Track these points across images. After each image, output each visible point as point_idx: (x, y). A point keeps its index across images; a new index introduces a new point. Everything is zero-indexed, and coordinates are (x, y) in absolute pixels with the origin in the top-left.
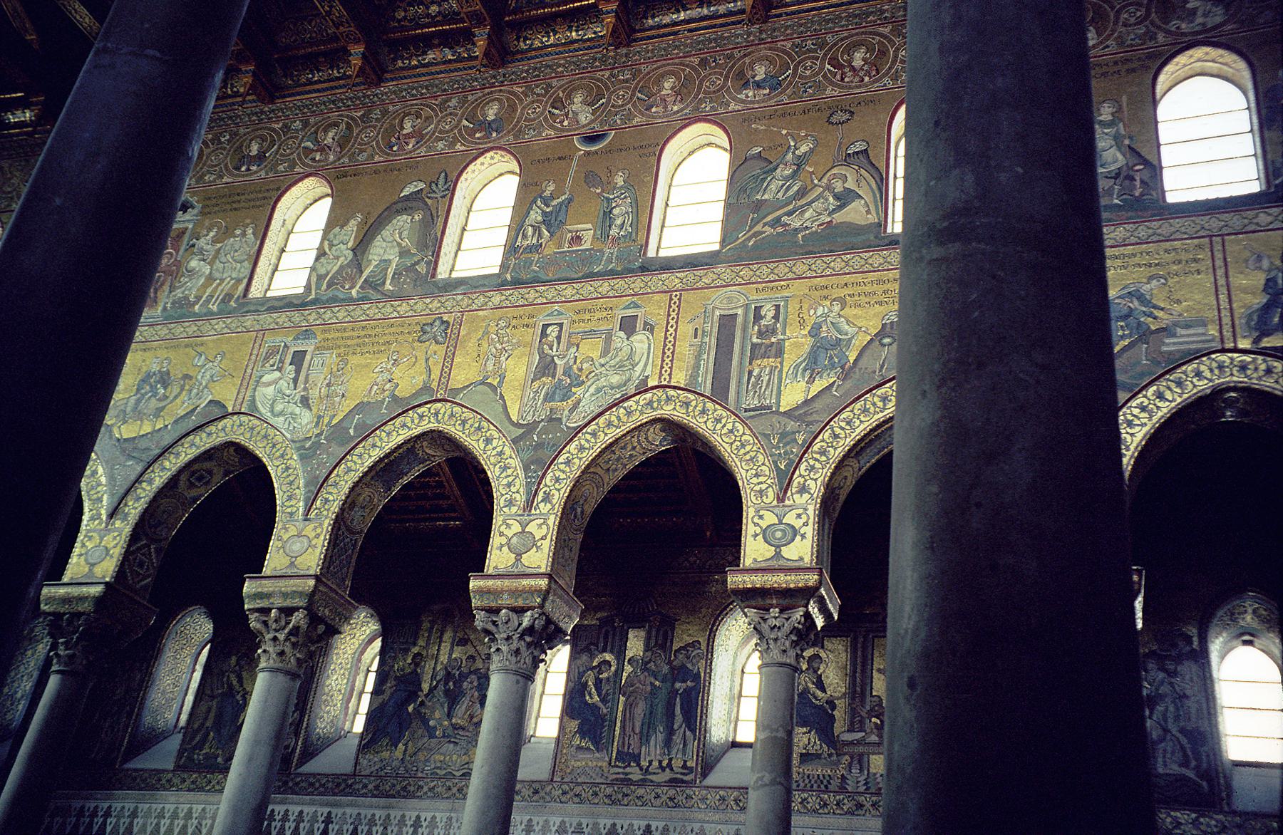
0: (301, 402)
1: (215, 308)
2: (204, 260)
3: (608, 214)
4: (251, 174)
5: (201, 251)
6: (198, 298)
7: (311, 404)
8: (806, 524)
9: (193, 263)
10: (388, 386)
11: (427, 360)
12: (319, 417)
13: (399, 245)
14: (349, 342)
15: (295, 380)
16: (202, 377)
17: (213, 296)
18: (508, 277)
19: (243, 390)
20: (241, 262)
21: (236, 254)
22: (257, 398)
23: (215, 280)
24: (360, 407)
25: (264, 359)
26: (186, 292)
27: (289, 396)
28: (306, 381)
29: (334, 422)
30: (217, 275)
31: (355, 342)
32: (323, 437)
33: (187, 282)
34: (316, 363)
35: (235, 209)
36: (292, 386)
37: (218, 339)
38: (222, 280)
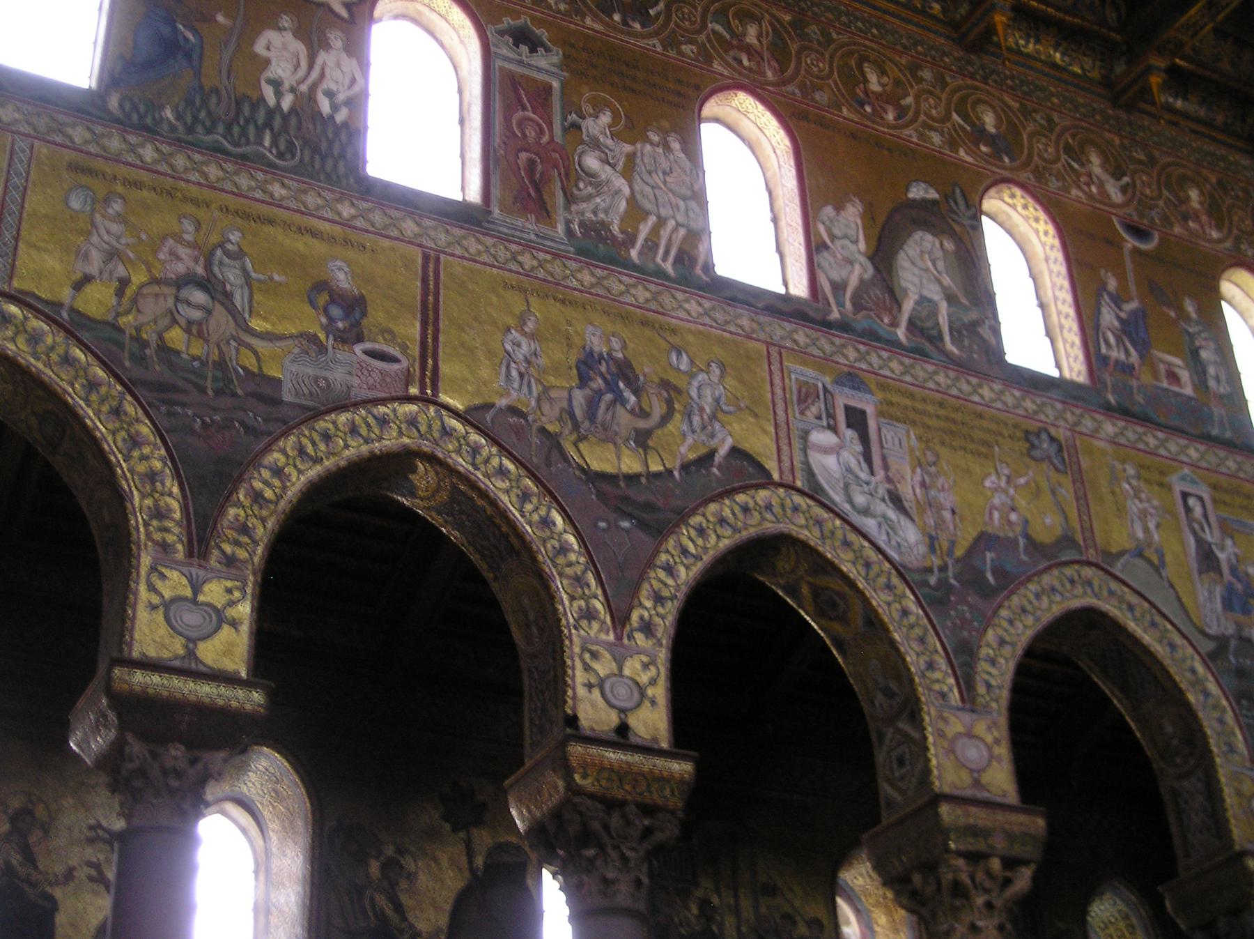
0: (892, 500)
1: (668, 267)
2: (613, 166)
3: (1195, 353)
4: (628, 34)
5: (596, 145)
6: (631, 240)
7: (909, 510)
8: (653, 682)
9: (592, 162)
10: (1013, 517)
11: (1053, 492)
12: (931, 538)
13: (939, 282)
14: (933, 422)
15: (867, 456)
16: (699, 396)
17: (657, 245)
18: (1112, 399)
19: (785, 448)
20: (684, 199)
21: (668, 179)
22: (816, 471)
23: (647, 213)
24: (985, 540)
25: (800, 402)
26: (602, 215)
27: (868, 483)
28: (886, 467)
29: (959, 552)
30: (648, 206)
31: (943, 424)
32: (950, 574)
33: (590, 197)
34: (889, 437)
35: (633, 90)
36: (864, 465)
37: (700, 333)
38: (661, 222)
